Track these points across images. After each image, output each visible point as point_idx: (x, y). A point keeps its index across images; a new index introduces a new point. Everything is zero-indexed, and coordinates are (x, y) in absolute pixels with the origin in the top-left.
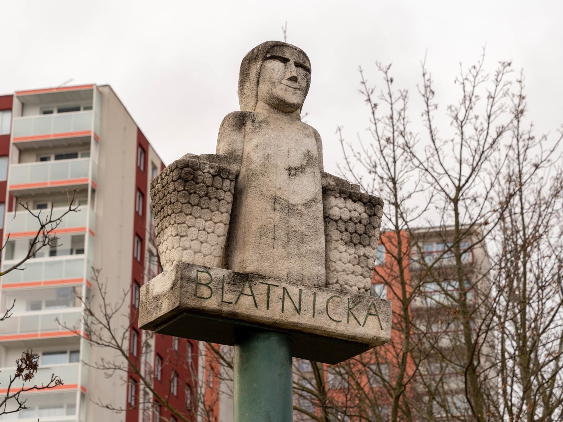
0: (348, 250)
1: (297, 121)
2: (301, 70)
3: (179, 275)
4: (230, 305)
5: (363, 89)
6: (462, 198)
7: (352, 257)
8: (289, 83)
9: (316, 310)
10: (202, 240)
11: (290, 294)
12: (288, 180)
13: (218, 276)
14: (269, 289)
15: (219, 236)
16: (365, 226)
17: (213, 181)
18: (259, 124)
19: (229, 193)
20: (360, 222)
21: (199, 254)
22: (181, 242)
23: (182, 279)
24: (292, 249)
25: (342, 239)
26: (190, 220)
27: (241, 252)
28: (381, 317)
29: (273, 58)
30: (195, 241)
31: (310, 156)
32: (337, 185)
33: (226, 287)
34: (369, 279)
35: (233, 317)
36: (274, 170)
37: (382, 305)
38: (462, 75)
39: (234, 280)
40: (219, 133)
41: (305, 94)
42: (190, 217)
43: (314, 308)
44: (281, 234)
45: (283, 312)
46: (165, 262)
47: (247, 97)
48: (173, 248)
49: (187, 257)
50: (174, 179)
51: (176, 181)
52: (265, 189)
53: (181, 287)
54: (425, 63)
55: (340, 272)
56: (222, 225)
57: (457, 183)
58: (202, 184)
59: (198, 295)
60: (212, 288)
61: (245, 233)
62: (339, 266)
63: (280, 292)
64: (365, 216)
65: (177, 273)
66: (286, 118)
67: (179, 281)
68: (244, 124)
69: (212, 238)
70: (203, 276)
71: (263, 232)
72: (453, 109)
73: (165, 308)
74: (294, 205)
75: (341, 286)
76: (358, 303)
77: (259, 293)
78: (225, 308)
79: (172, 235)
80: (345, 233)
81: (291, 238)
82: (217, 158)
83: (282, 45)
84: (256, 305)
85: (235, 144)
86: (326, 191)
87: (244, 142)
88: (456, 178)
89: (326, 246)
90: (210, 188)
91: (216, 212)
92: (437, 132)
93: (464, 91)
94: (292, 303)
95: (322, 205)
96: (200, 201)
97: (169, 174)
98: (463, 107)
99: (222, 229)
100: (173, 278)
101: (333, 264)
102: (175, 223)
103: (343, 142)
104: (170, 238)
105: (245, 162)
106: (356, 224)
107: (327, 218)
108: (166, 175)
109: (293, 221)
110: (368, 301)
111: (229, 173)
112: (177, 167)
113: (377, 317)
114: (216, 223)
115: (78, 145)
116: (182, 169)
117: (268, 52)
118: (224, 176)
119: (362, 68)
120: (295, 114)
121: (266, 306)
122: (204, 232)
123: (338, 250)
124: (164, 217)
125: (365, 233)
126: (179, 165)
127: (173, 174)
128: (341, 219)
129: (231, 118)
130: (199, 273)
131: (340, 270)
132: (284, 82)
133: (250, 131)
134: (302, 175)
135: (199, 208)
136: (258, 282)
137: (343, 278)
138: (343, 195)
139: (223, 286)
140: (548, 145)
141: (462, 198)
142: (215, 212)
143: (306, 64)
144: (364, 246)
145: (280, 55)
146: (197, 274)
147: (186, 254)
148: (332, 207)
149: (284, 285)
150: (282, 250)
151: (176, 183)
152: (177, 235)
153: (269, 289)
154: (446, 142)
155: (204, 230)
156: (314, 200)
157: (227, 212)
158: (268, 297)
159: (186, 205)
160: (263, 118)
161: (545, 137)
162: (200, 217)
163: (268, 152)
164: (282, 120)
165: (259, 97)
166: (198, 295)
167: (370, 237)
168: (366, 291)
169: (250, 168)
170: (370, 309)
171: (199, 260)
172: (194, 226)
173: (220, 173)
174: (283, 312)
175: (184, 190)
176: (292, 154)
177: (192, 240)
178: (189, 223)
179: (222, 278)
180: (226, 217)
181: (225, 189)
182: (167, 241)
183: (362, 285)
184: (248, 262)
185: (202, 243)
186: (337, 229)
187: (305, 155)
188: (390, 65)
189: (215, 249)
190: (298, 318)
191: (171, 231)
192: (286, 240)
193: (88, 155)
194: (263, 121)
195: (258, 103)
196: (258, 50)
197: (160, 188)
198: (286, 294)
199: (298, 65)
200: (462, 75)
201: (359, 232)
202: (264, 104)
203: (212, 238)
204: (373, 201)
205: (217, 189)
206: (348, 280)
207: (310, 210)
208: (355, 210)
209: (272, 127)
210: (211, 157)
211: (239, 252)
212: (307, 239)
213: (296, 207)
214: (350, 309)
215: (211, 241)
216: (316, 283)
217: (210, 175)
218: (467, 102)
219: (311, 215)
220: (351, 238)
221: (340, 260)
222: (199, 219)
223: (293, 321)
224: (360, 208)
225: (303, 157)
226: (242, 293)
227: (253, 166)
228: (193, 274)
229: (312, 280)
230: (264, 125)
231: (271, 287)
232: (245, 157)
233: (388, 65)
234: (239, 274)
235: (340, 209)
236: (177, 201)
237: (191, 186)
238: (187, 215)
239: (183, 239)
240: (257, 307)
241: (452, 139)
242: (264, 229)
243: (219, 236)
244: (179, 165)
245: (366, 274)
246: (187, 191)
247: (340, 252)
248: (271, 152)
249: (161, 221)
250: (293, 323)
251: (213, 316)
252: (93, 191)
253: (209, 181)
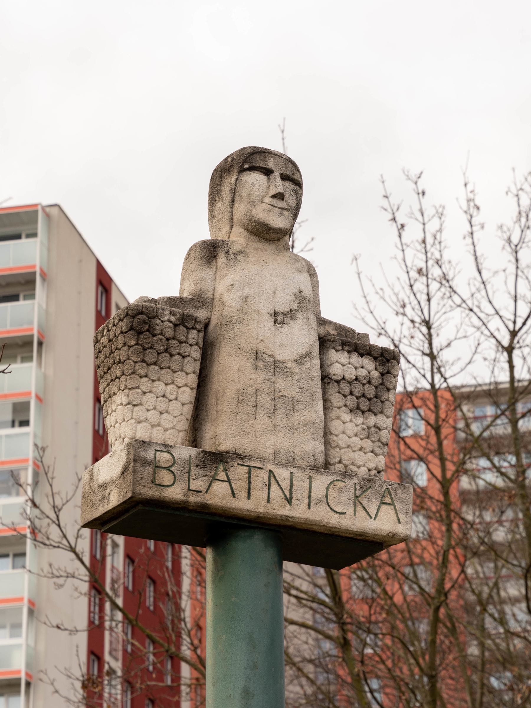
0: (354, 420)
1: (285, 252)
3: (132, 457)
4: (199, 494)
5: (386, 206)
6: (518, 346)
7: (359, 428)
8: (274, 201)
9: (312, 499)
10: (161, 410)
11: (278, 479)
12: (273, 328)
13: (183, 457)
14: (250, 473)
15: (183, 404)
16: (376, 387)
17: (175, 332)
19: (196, 347)
20: (369, 382)
21: (158, 428)
22: (134, 413)
23: (135, 461)
24: (280, 420)
25: (345, 406)
26: (145, 384)
27: (212, 425)
28: (398, 506)
30: (152, 411)
31: (302, 296)
32: (339, 334)
33: (194, 471)
34: (382, 457)
36: (255, 316)
37: (399, 491)
38: (515, 184)
39: (204, 462)
40: (183, 269)
41: (295, 216)
42: (146, 379)
43: (310, 497)
44: (265, 400)
45: (268, 502)
46: (113, 440)
47: (219, 220)
48: (124, 420)
50: (124, 330)
51: (126, 333)
52: (243, 341)
53: (134, 472)
54: (466, 169)
55: (344, 448)
56: (187, 389)
57: (511, 327)
58: (160, 337)
59: (157, 482)
60: (175, 472)
61: (217, 400)
62: (342, 440)
63: (264, 476)
64: (375, 374)
65: (128, 453)
66: (270, 248)
67: (132, 464)
68: (215, 256)
69: (175, 407)
70: (164, 457)
71: (241, 398)
72: (505, 229)
74: (282, 362)
75: (346, 466)
76: (368, 489)
77: (237, 477)
78: (193, 499)
79: (122, 404)
80: (350, 397)
81: (279, 405)
82: (180, 301)
83: (264, 152)
84: (233, 494)
85: (203, 283)
87: (215, 280)
88: (510, 320)
89: (325, 414)
90: (171, 342)
91: (180, 373)
92: (485, 259)
93: (519, 205)
94: (280, 491)
95: (319, 361)
96: (158, 358)
97: (118, 323)
98: (517, 226)
100: (124, 460)
101: (335, 438)
102: (126, 388)
103: (361, 275)
104: (119, 407)
105: (217, 307)
106: (364, 385)
107: (325, 378)
108: (114, 325)
109: (281, 383)
110: (381, 486)
111: (196, 321)
112: (127, 315)
113: (392, 507)
114: (179, 387)
115: (19, 284)
116: (134, 317)
117: (245, 161)
118: (190, 326)
119: (385, 178)
120: (282, 242)
121: (246, 494)
122: (164, 399)
123: (341, 420)
124: (112, 380)
125: (376, 397)
126: (130, 312)
127: (123, 323)
128: (344, 378)
129: (198, 249)
130: (158, 453)
131: (344, 446)
132: (267, 200)
133: (223, 266)
134: (292, 322)
135: (157, 368)
136: (235, 464)
137: (347, 456)
138: (347, 348)
139: (190, 469)
141: (518, 346)
142: (177, 373)
143: (296, 177)
144: (375, 414)
145: (261, 165)
146: (155, 454)
147: (141, 428)
148: (332, 363)
149: (270, 466)
150: (267, 421)
151: (127, 335)
152: (129, 404)
153: (250, 473)
154: (496, 272)
155: (164, 396)
156: (308, 355)
157: (194, 373)
158: (250, 483)
159: (140, 364)
160: (240, 248)
162: (159, 380)
163: (246, 292)
164: (265, 250)
165: (234, 220)
166: (157, 482)
167: (382, 402)
168: (379, 472)
169: (224, 314)
170: (384, 496)
171: (157, 436)
172: (150, 392)
174: (268, 502)
175: (137, 344)
176: (278, 295)
177: (148, 410)
179: (188, 459)
180: (192, 379)
181: (191, 341)
182: (115, 411)
183: (372, 465)
184: (223, 438)
185: (161, 413)
186: (339, 392)
187: (295, 296)
188: (421, 173)
189: (179, 421)
190: (289, 510)
191: (120, 398)
192: (272, 407)
193: (32, 296)
194: (241, 252)
195: (234, 229)
196: (233, 159)
197: (106, 343)
198: (272, 479)
199: (284, 178)
200: (515, 184)
201: (369, 396)
202: (241, 230)
203: (175, 407)
204: (386, 355)
205: (181, 343)
206: (355, 458)
207: (303, 368)
208: (362, 367)
209: (252, 259)
210: (172, 301)
211: (210, 425)
212: (300, 406)
213: (284, 365)
214: (357, 497)
215: (173, 410)
216: (312, 463)
217: (171, 324)
218: (523, 220)
219: (304, 375)
220: (358, 403)
221: (344, 433)
222: (157, 383)
223: (283, 513)
224: (369, 364)
225: (293, 298)
226: (214, 479)
227: (227, 312)
228: (150, 455)
229: (307, 459)
230: (241, 257)
231: (253, 470)
232: (216, 300)
233: (419, 172)
234: (210, 453)
235: (343, 365)
236: (128, 359)
237: (146, 338)
238: (141, 377)
239: (136, 408)
240: (234, 496)
241: (503, 268)
242: (243, 394)
243: (183, 404)
244: (130, 312)
245: (377, 450)
246: (141, 345)
247: (344, 423)
248: (251, 293)
249: (108, 385)
250: (282, 516)
251: (178, 509)
252: (40, 344)
253: (169, 333)
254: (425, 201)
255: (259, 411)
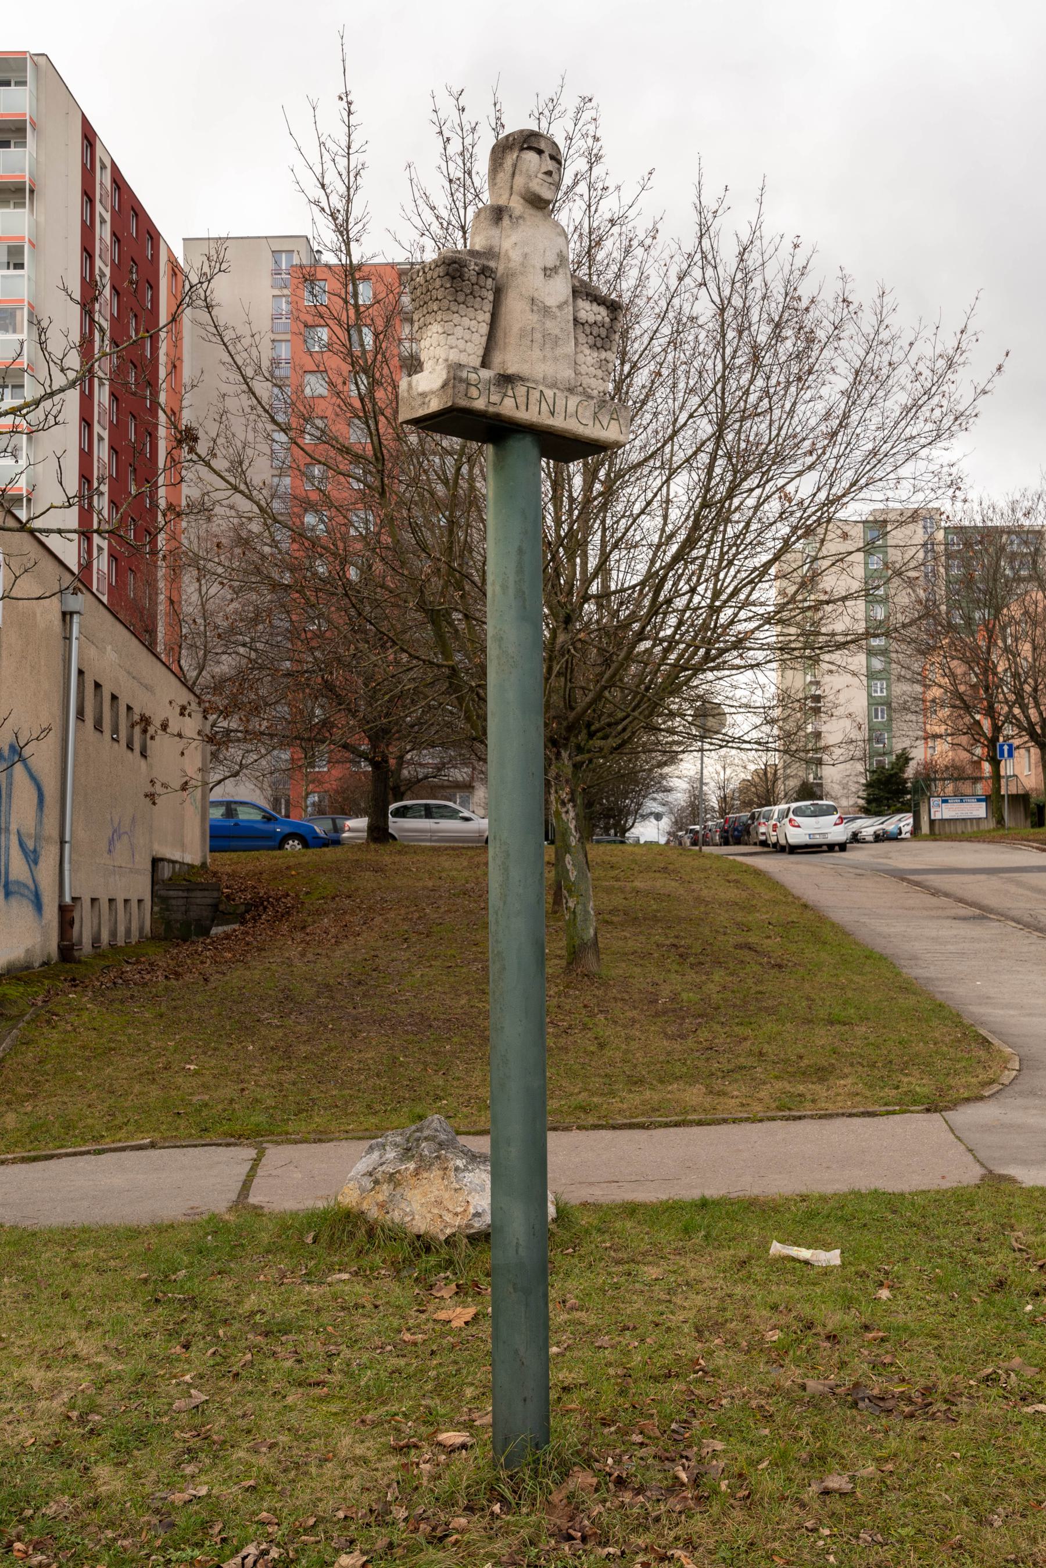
2: (554, 163)
5: (435, 120)
8: (545, 177)
18: (517, 220)
24: (548, 352)
29: (530, 148)
33: (492, 388)
35: (498, 417)
44: (538, 336)
49: (454, 356)
53: (454, 387)
62: (583, 369)
64: (607, 319)
66: (539, 214)
69: (476, 336)
70: (473, 376)
73: (434, 405)
78: (491, 409)
86: (575, 293)
99: (484, 329)
100: (445, 377)
105: (502, 260)
107: (575, 320)
109: (549, 324)
115: (10, 130)
132: (540, 175)
137: (586, 381)
140: (627, 199)
149: (541, 388)
156: (566, 303)
161: (618, 188)
171: (464, 359)
173: (485, 271)
176: (548, 253)
178: (455, 322)
180: (487, 317)
191: (436, 328)
193: (23, 144)
194: (520, 217)
199: (552, 158)
203: (476, 336)
212: (560, 342)
224: (603, 311)
226: (505, 395)
227: (512, 265)
228: (464, 375)
230: (521, 221)
237: (458, 283)
252: (32, 191)
253: (474, 279)
254: (465, 117)
255: (535, 345)
